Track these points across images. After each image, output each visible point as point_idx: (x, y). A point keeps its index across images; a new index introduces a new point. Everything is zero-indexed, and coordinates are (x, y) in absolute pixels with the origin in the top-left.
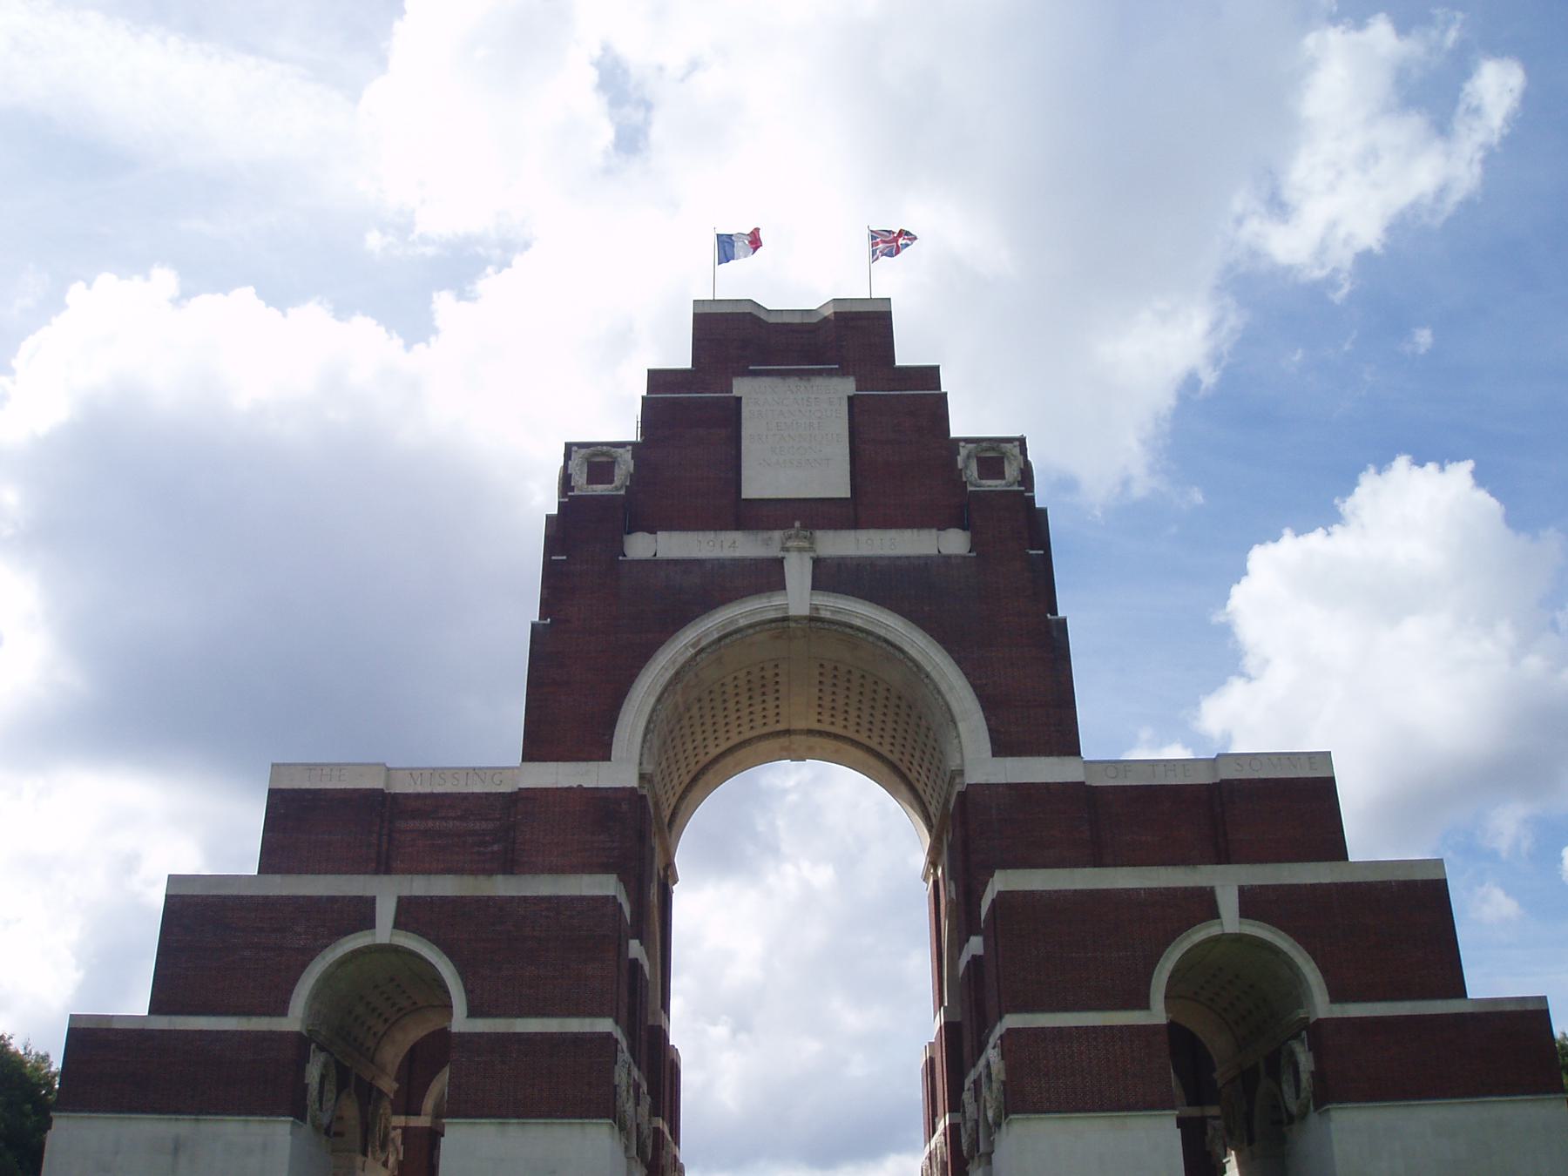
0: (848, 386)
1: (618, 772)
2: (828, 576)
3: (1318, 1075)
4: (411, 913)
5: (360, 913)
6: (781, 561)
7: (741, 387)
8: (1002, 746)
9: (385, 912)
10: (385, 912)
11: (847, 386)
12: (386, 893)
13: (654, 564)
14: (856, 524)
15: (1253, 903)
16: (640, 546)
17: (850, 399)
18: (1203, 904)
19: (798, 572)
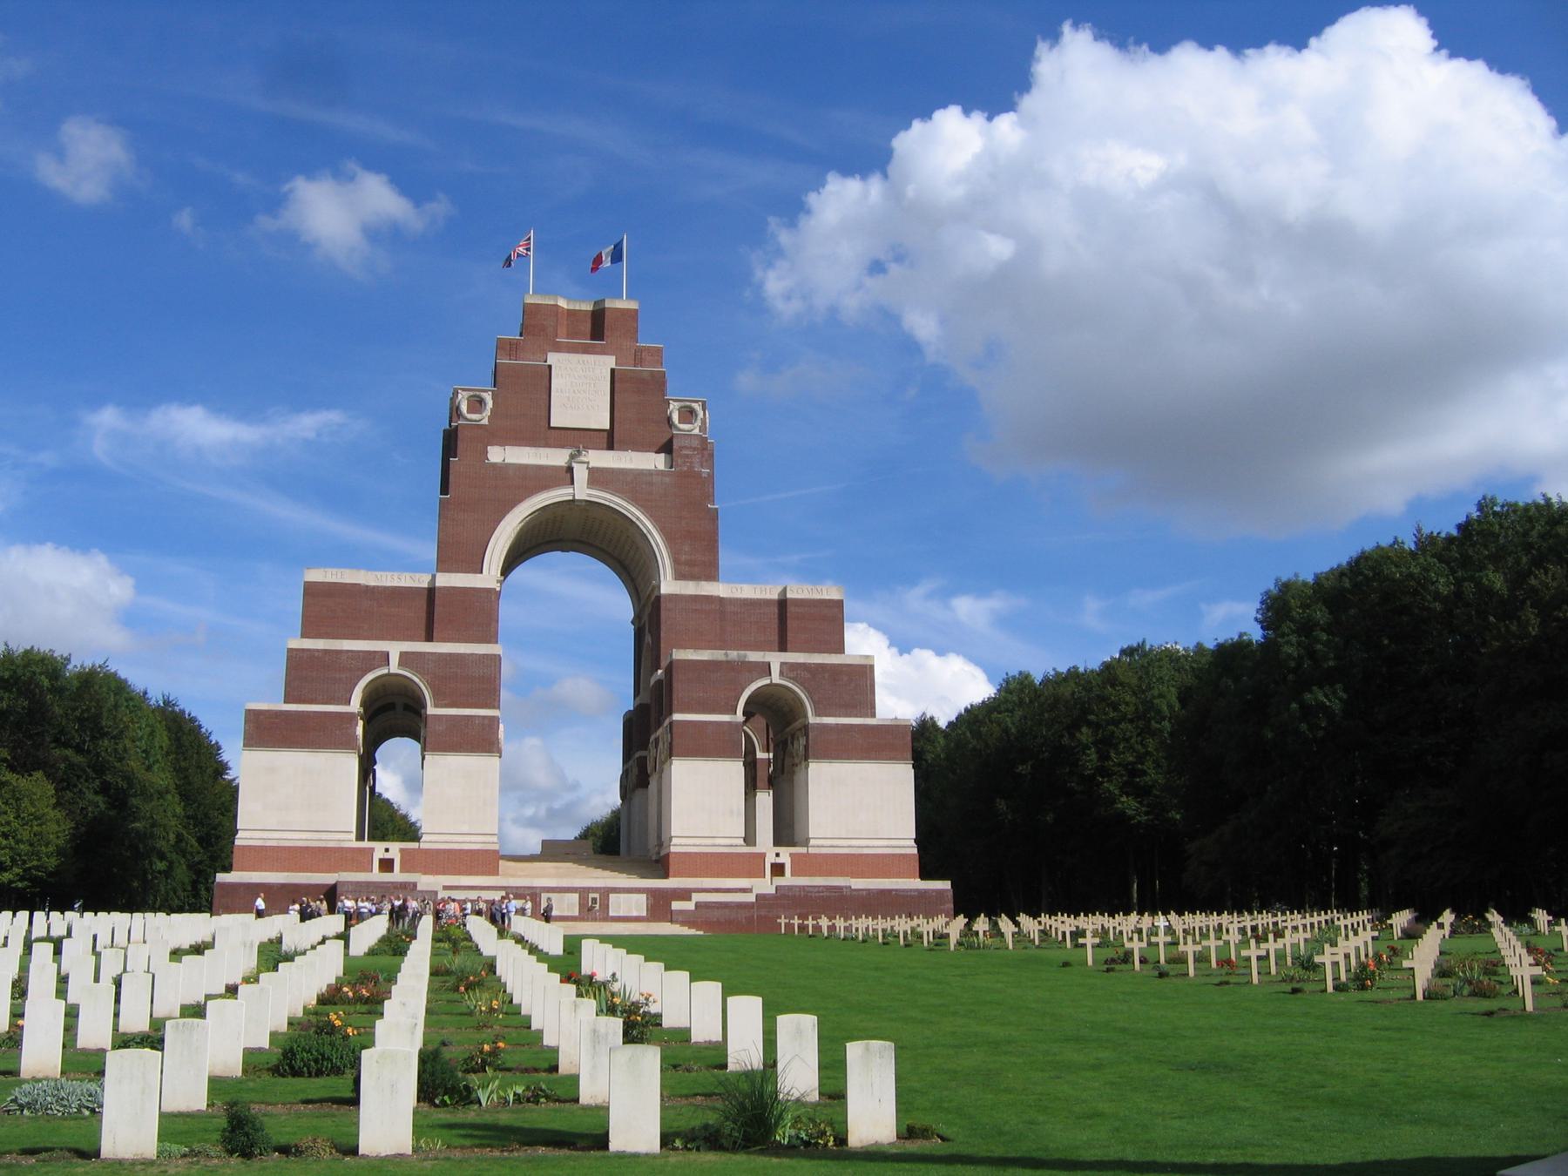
0: (610, 362)
1: (489, 577)
2: (598, 477)
3: (806, 747)
4: (405, 658)
5: (385, 658)
6: (570, 470)
7: (553, 358)
8: (679, 576)
9: (394, 660)
10: (394, 660)
11: (610, 362)
12: (395, 649)
13: (503, 468)
14: (610, 446)
15: (787, 669)
16: (496, 455)
17: (613, 371)
18: (766, 669)
19: (581, 474)
